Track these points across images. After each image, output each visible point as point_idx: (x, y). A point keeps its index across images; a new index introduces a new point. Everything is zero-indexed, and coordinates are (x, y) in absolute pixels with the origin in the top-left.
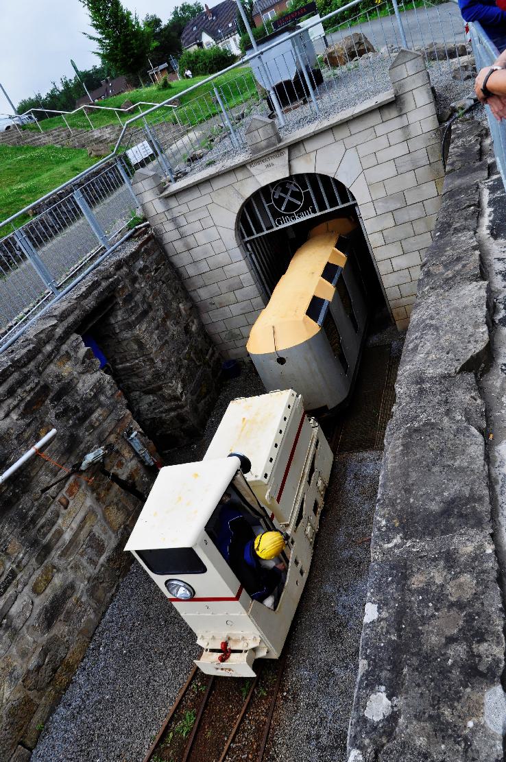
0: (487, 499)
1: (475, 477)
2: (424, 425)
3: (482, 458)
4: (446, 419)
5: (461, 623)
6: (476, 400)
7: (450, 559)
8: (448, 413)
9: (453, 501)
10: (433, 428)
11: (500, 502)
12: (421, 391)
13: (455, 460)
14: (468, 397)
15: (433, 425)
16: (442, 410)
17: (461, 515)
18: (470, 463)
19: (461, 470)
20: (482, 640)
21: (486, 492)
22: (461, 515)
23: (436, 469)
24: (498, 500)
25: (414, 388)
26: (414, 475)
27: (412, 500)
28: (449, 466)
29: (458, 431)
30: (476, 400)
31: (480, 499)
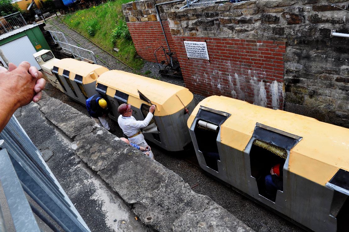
0: (105, 180)
1: (115, 183)
2: (158, 186)
3: (118, 191)
4: (150, 196)
5: (90, 151)
6: (148, 219)
7: (103, 158)
8: (153, 200)
9: (117, 172)
10: (152, 188)
11: (109, 192)
12: (181, 200)
13: (128, 183)
14: (152, 216)
15: (153, 189)
16: (157, 200)
17: (110, 170)
18: (121, 186)
19: (123, 181)
20: (83, 152)
21: (107, 181)
22: (110, 170)
23: (133, 175)
24: (110, 192)
25: (186, 198)
26: (139, 167)
27: (131, 162)
28: (129, 179)
29: (138, 194)
30: (148, 219)
31: (107, 178)
